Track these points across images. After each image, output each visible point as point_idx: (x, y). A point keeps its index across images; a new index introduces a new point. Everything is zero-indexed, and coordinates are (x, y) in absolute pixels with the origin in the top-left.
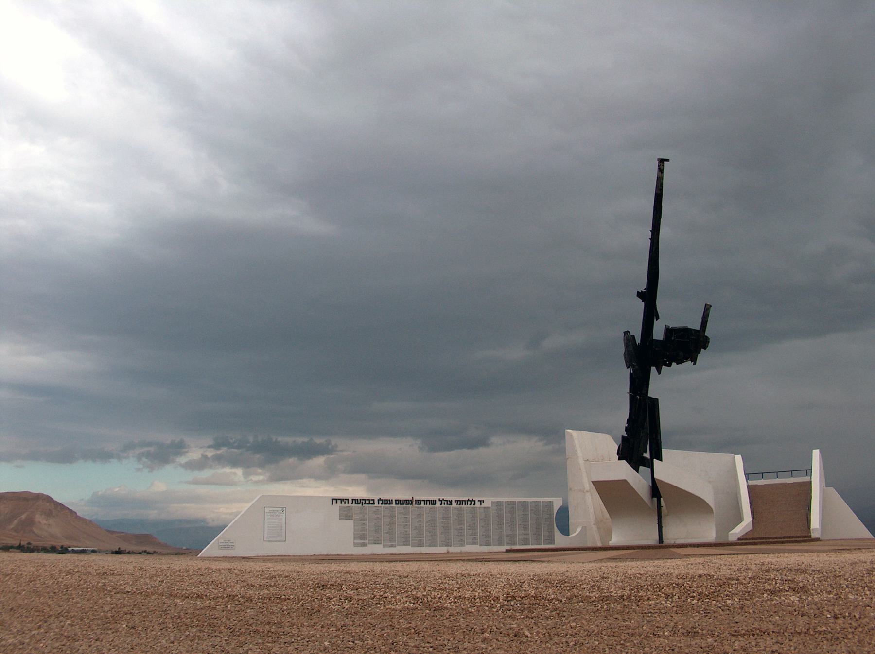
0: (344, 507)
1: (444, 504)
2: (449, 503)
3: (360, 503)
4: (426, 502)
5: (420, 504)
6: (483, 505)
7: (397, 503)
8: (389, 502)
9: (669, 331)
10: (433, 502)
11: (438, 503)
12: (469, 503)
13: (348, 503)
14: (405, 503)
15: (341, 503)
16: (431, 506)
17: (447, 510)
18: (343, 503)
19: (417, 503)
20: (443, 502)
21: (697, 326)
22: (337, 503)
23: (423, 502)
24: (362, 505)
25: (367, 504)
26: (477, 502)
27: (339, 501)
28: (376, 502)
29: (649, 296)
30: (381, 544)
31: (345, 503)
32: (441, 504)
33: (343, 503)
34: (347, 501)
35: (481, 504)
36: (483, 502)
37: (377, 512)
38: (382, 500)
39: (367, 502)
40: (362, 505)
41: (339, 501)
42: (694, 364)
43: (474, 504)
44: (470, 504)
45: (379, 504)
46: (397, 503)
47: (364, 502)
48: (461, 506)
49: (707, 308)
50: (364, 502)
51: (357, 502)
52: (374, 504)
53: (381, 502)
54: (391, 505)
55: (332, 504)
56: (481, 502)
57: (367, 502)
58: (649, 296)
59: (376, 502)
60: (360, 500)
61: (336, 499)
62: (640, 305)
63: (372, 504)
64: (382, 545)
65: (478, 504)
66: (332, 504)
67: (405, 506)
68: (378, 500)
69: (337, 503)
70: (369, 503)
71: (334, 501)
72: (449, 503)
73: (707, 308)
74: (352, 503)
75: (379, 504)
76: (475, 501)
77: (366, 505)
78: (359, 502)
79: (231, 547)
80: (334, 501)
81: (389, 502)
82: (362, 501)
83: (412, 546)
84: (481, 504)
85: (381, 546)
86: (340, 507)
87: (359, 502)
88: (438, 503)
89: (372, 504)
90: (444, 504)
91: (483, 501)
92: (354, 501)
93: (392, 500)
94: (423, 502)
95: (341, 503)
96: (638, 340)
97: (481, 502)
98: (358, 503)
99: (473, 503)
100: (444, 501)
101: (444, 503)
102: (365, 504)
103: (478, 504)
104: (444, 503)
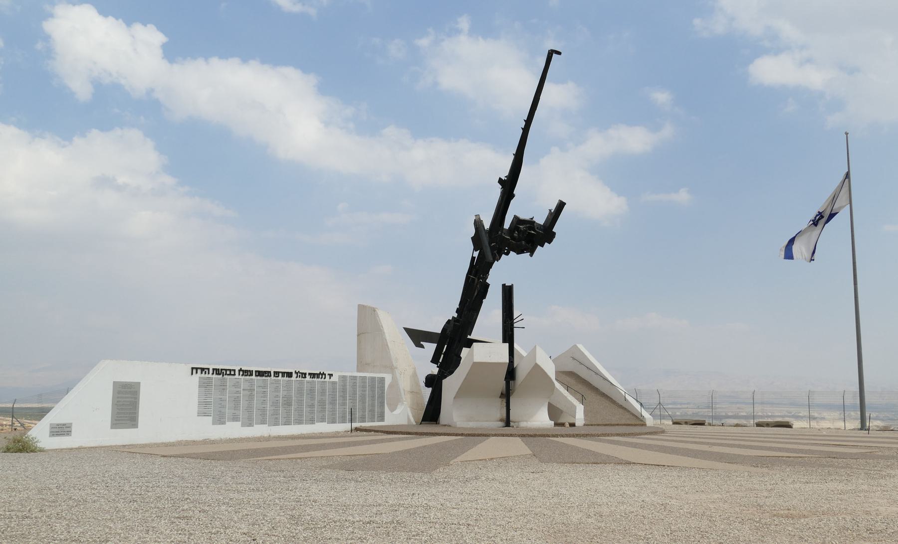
0: (204, 378)
1: (300, 377)
2: (303, 376)
4: (283, 373)
5: (278, 376)
6: (333, 379)
9: (517, 221)
10: (289, 375)
11: (294, 375)
12: (320, 376)
13: (209, 373)
15: (202, 373)
16: (287, 379)
17: (301, 383)
18: (204, 372)
21: (541, 220)
22: (197, 373)
23: (280, 375)
24: (223, 376)
25: (228, 375)
26: (327, 375)
27: (199, 371)
28: (237, 373)
29: (509, 185)
30: (240, 421)
31: (205, 373)
32: (297, 377)
33: (204, 372)
35: (330, 378)
36: (332, 376)
37: (237, 385)
38: (243, 371)
40: (223, 376)
41: (199, 371)
42: (531, 256)
43: (325, 378)
44: (322, 378)
45: (239, 375)
48: (313, 379)
49: (561, 205)
52: (234, 375)
53: (241, 373)
54: (251, 377)
55: (192, 374)
56: (331, 375)
57: (228, 372)
58: (509, 185)
59: (237, 373)
61: (197, 369)
62: (498, 190)
63: (233, 375)
65: (328, 377)
66: (192, 374)
67: (264, 378)
69: (197, 373)
70: (230, 374)
71: (194, 371)
72: (303, 376)
73: (561, 205)
74: (213, 374)
76: (325, 374)
79: (66, 433)
80: (194, 371)
83: (269, 426)
84: (330, 378)
85: (239, 423)
86: (200, 377)
88: (294, 375)
89: (233, 375)
90: (300, 377)
91: (332, 375)
94: (280, 375)
95: (202, 373)
96: (487, 225)
97: (331, 375)
99: (324, 376)
100: (300, 373)
101: (300, 376)
103: (328, 377)
104: (300, 376)
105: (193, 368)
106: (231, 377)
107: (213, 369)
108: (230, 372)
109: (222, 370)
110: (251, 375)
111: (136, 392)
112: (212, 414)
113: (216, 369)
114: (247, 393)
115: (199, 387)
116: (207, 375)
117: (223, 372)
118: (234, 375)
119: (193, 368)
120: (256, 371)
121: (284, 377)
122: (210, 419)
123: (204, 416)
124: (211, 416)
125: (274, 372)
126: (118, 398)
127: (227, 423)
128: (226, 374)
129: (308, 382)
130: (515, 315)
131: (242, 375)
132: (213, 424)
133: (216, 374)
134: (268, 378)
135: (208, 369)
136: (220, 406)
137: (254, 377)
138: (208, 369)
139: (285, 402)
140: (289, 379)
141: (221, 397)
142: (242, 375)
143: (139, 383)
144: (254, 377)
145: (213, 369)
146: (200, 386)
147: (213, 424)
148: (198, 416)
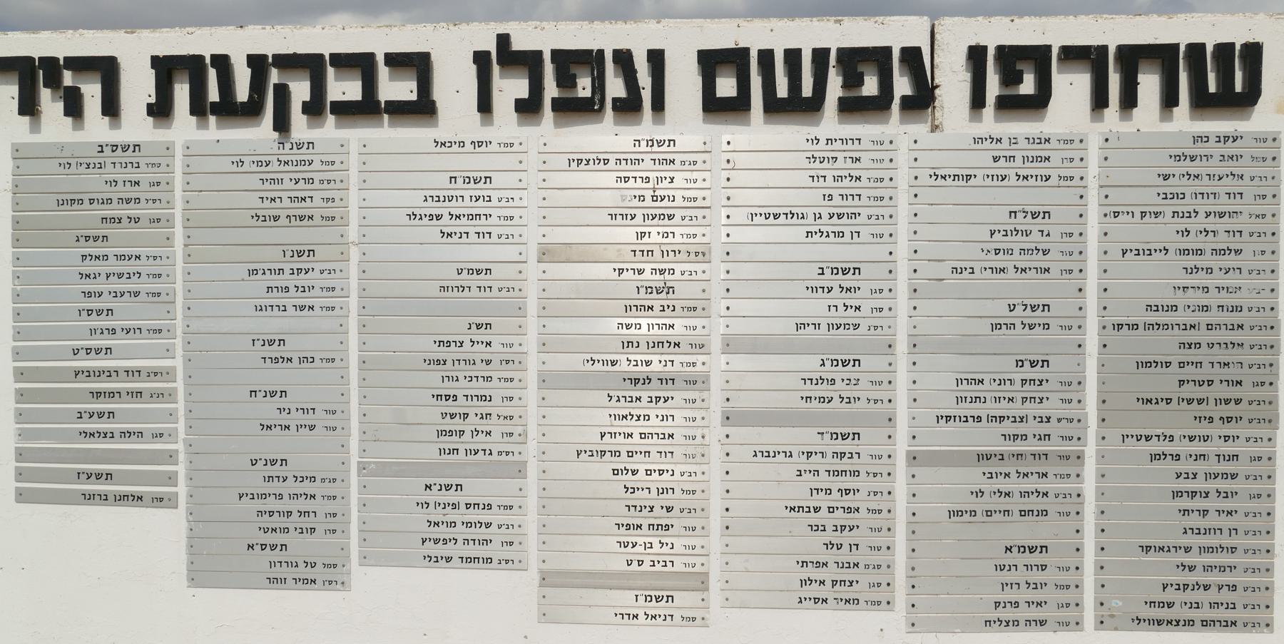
0: (67, 159)
3: (252, 110)
5: (1040, 100)
7: (726, 87)
8: (615, 87)
13: (111, 107)
14: (834, 86)
19: (993, 87)
24: (282, 125)
25: (344, 110)
31: (74, 107)
33: (51, 106)
34: (92, 92)
38: (529, 62)
39: (344, 88)
40: (282, 125)
45: (485, 105)
46: (726, 87)
47: (300, 90)
50: (300, 90)
51: (213, 95)
60: (258, 63)
63: (398, 110)
68: (481, 59)
74: (161, 109)
75: (485, 105)
77: (330, 130)
78: (242, 93)
81: (615, 87)
82: (274, 76)
87: (242, 93)
89: (398, 110)
92: (182, 93)
93: (656, 58)
98: (229, 110)
102: (314, 108)
107: (166, 68)
112: (182, 489)
113: (193, 66)
115: (16, 242)
117: (282, 93)
121: (1129, 100)
123: (89, 498)
127: (360, 575)
128: (314, 108)
131: (528, 108)
132: (199, 576)
133: (199, 108)
135: (107, 70)
136: (267, 412)
139: (1163, 383)
140: (1020, 127)
141: (272, 325)
145: (166, 68)
146: (23, 233)
147: (199, 576)
148: (21, 496)
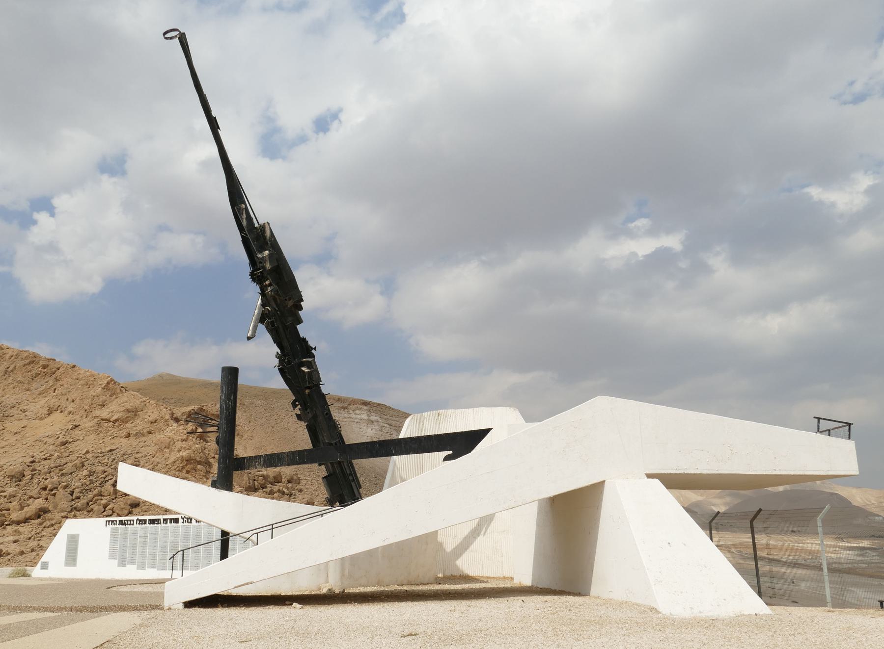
2: (189, 521)
16: (175, 524)
17: (187, 528)
20: (185, 519)
22: (109, 524)
23: (169, 521)
30: (135, 564)
31: (114, 524)
32: (183, 522)
37: (135, 533)
41: (110, 523)
45: (137, 524)
52: (133, 524)
54: (146, 526)
55: (106, 525)
64: (136, 566)
66: (106, 525)
67: (156, 525)
70: (130, 524)
72: (189, 521)
74: (119, 524)
80: (108, 523)
85: (135, 566)
86: (111, 528)
88: (181, 520)
90: (185, 522)
94: (169, 521)
95: (112, 524)
105: (106, 521)
106: (131, 526)
107: (119, 521)
108: (130, 522)
109: (125, 521)
110: (145, 523)
111: (69, 542)
114: (142, 539)
116: (115, 526)
118: (133, 524)
119: (106, 521)
120: (149, 520)
122: (116, 562)
124: (116, 559)
125: (163, 519)
126: (69, 545)
127: (127, 565)
128: (128, 524)
129: (194, 527)
130: (237, 423)
134: (159, 525)
135: (116, 521)
137: (147, 525)
138: (116, 521)
139: (172, 548)
142: (139, 524)
143: (78, 535)
144: (147, 525)
148: (109, 559)
